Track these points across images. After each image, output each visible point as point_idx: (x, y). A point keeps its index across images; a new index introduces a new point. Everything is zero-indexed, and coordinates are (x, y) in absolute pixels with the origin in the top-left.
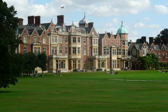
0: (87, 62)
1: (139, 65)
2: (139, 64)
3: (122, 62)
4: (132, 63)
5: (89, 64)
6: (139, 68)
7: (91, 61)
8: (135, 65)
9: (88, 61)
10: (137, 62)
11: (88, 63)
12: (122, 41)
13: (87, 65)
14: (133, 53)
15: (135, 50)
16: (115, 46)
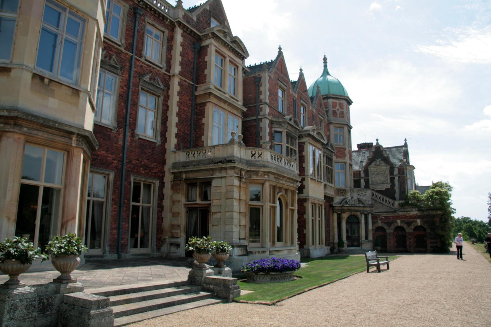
0: (161, 197)
1: (409, 230)
2: (409, 224)
3: (335, 216)
4: (373, 223)
5: (175, 210)
6: (411, 241)
7: (191, 184)
8: (390, 230)
9: (168, 191)
10: (398, 217)
11: (166, 203)
12: (331, 127)
13: (160, 219)
14: (372, 178)
15: (385, 168)
16: (318, 133)
